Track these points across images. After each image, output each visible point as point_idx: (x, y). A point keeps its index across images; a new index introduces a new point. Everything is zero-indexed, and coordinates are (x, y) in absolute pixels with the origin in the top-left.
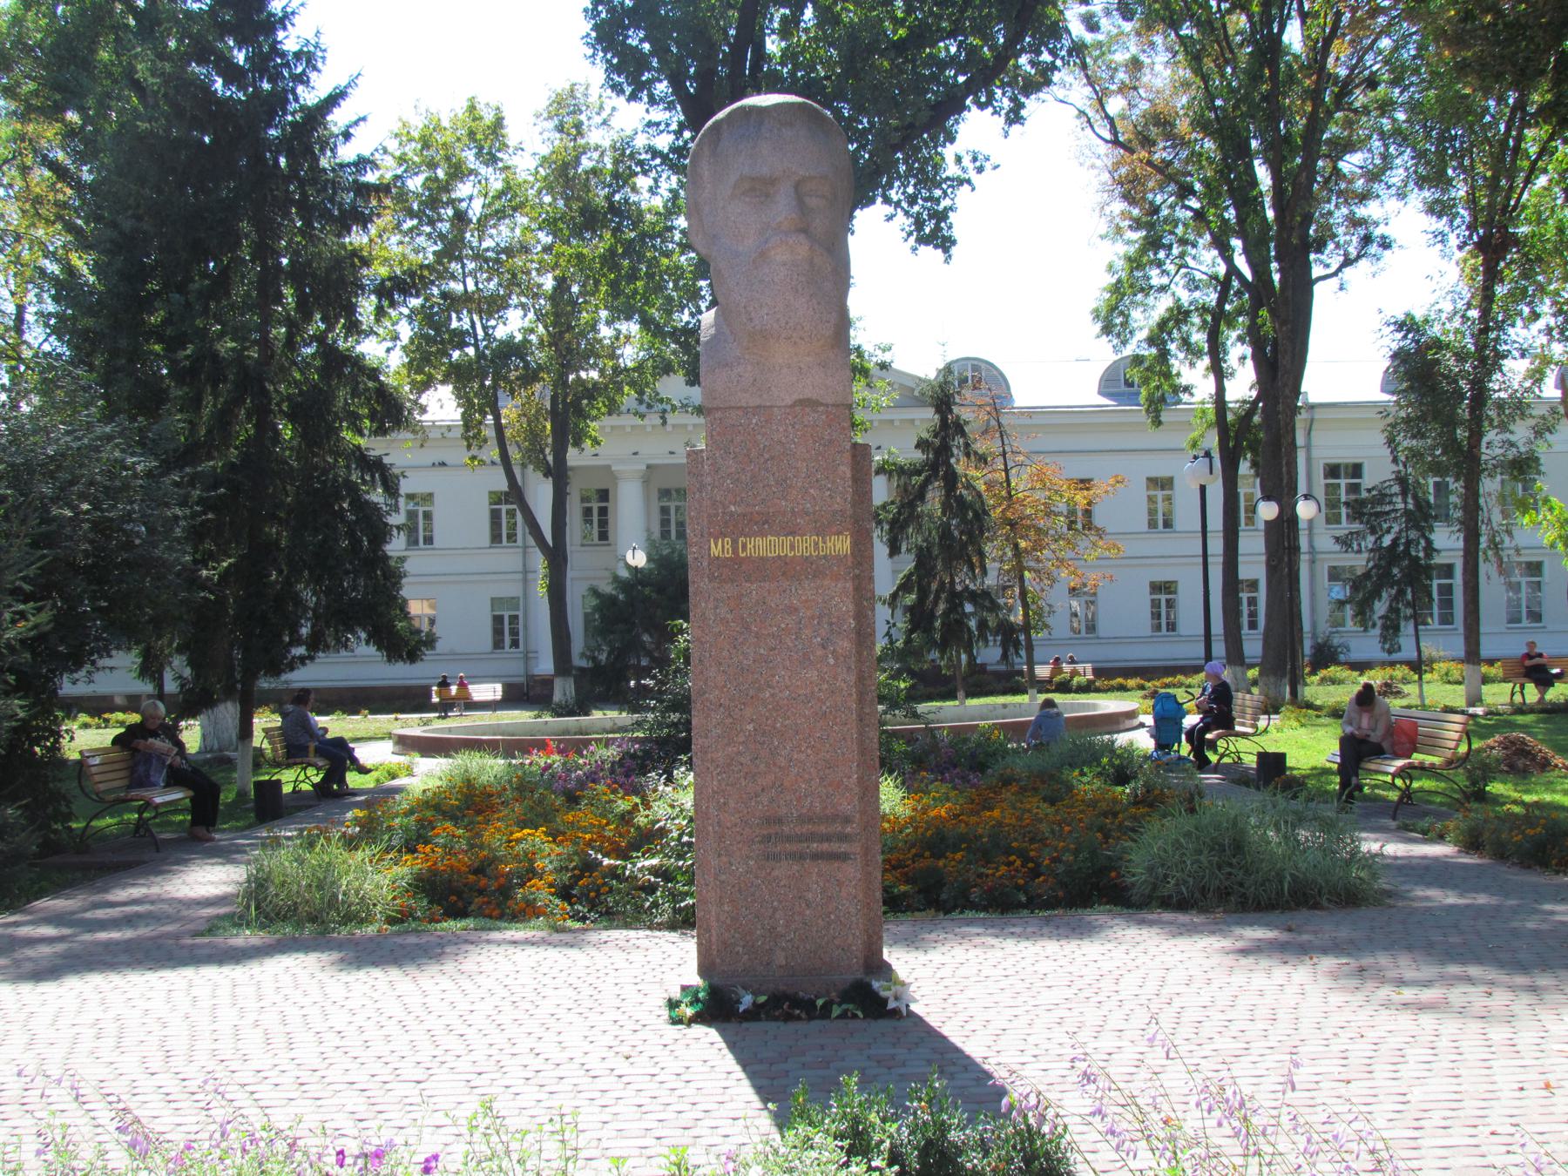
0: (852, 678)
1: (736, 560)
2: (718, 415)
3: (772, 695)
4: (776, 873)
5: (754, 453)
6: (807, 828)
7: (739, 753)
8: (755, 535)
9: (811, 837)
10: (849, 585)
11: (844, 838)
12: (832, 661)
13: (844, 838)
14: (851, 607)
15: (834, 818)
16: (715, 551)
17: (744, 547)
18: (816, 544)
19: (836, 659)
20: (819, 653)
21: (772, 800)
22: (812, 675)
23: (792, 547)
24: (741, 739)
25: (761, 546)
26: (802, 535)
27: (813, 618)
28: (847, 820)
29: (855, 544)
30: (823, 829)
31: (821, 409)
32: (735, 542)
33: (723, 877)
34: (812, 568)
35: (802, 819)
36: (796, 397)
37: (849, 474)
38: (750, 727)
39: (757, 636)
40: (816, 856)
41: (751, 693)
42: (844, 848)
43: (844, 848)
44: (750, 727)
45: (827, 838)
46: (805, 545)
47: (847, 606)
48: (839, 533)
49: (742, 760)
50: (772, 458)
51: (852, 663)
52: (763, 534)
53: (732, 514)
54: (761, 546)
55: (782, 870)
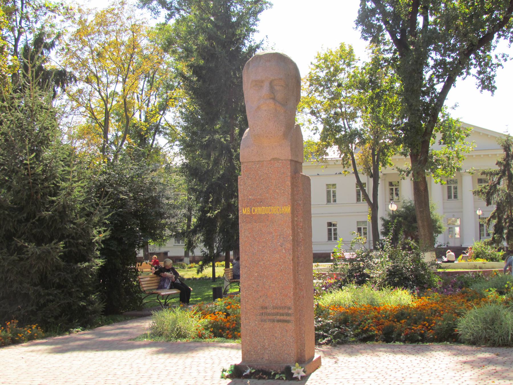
0: (291, 257)
3: (264, 263)
4: (265, 326)
5: (257, 177)
6: (276, 311)
7: (252, 284)
8: (258, 206)
9: (277, 314)
11: (288, 315)
12: (284, 251)
13: (288, 315)
14: (291, 232)
15: (285, 307)
18: (279, 209)
19: (285, 250)
20: (280, 248)
21: (263, 300)
22: (278, 256)
23: (270, 211)
24: (253, 278)
27: (277, 236)
28: (289, 308)
30: (281, 311)
31: (280, 161)
32: (251, 209)
33: (247, 327)
35: (274, 308)
36: (271, 157)
37: (290, 184)
38: (256, 274)
39: (258, 242)
40: (279, 321)
41: (256, 262)
42: (288, 318)
43: (288, 318)
44: (256, 274)
45: (282, 315)
48: (286, 206)
49: (253, 286)
50: (264, 179)
52: (260, 206)
53: (250, 199)
55: (267, 325)
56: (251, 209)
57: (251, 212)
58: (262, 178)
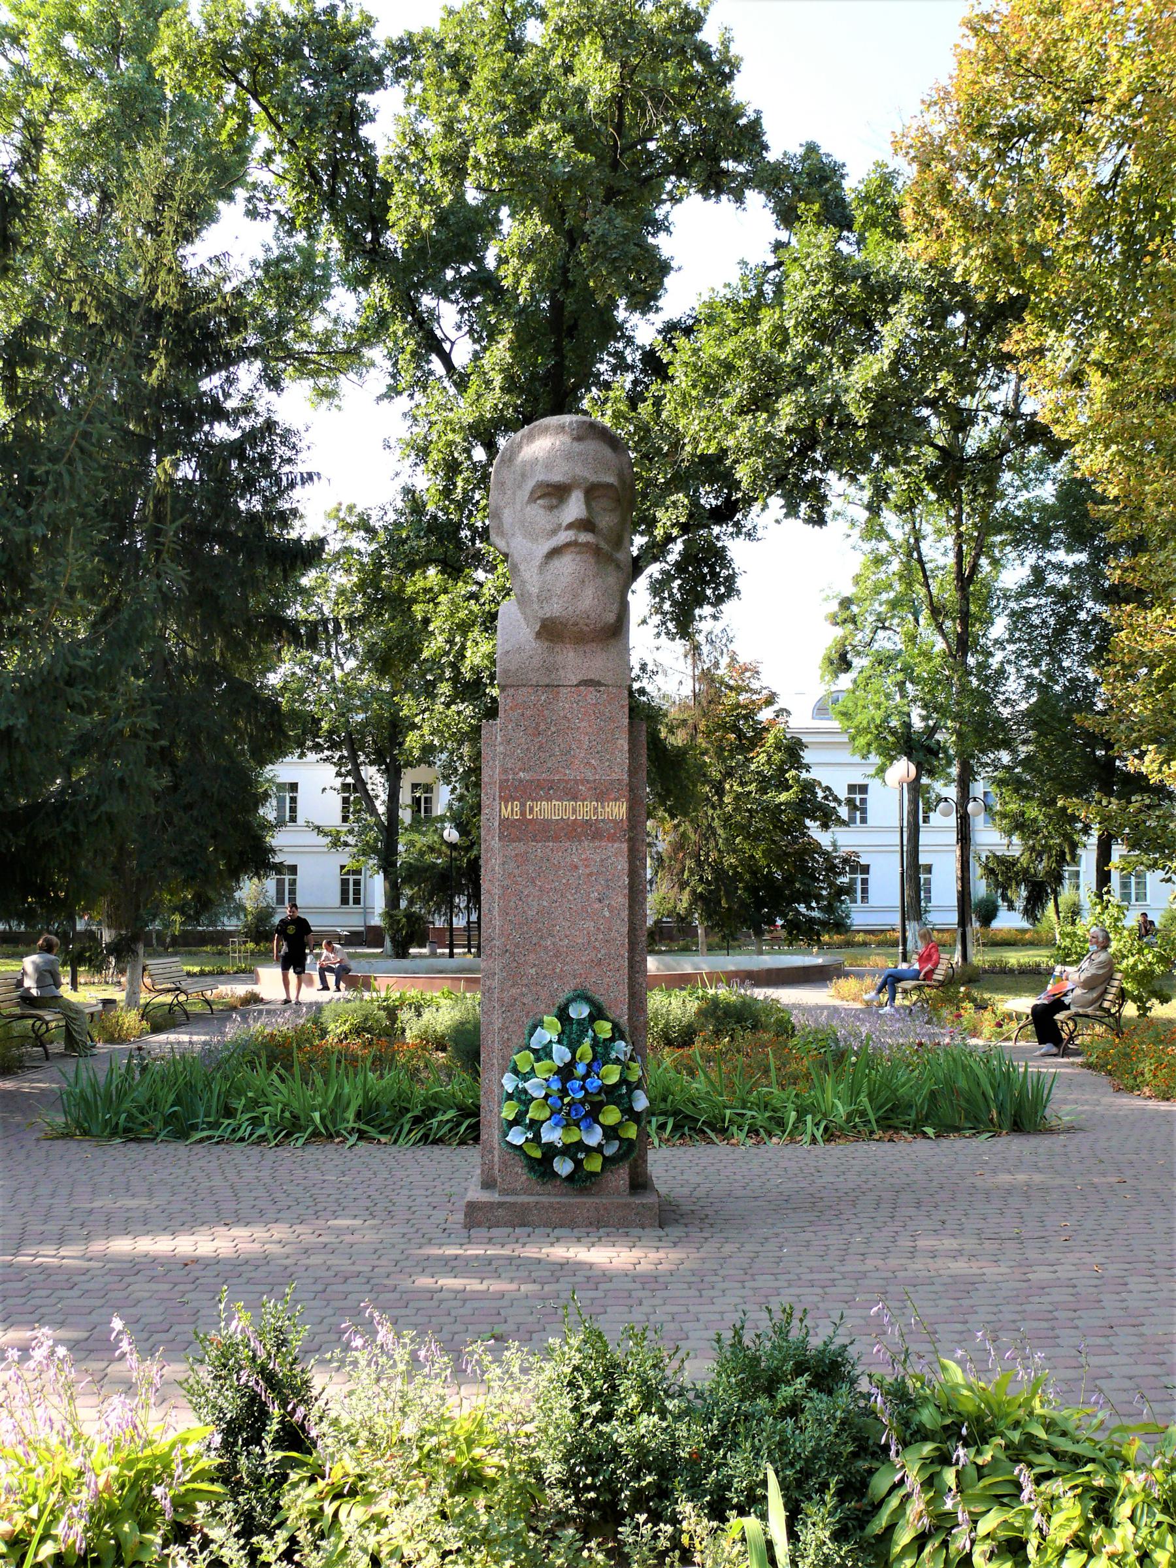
1: (524, 821)
2: (511, 691)
5: (542, 727)
10: (625, 846)
12: (607, 914)
14: (626, 866)
16: (505, 813)
17: (531, 809)
20: (597, 906)
23: (574, 811)
25: (547, 810)
26: (584, 800)
27: (591, 874)
29: (630, 809)
32: (523, 805)
34: (592, 831)
36: (580, 677)
37: (626, 748)
41: (535, 940)
44: (533, 971)
46: (585, 810)
47: (623, 865)
48: (616, 800)
51: (625, 914)
52: (549, 799)
53: (521, 781)
54: (547, 810)
56: (523, 805)
57: (523, 813)
58: (553, 729)
